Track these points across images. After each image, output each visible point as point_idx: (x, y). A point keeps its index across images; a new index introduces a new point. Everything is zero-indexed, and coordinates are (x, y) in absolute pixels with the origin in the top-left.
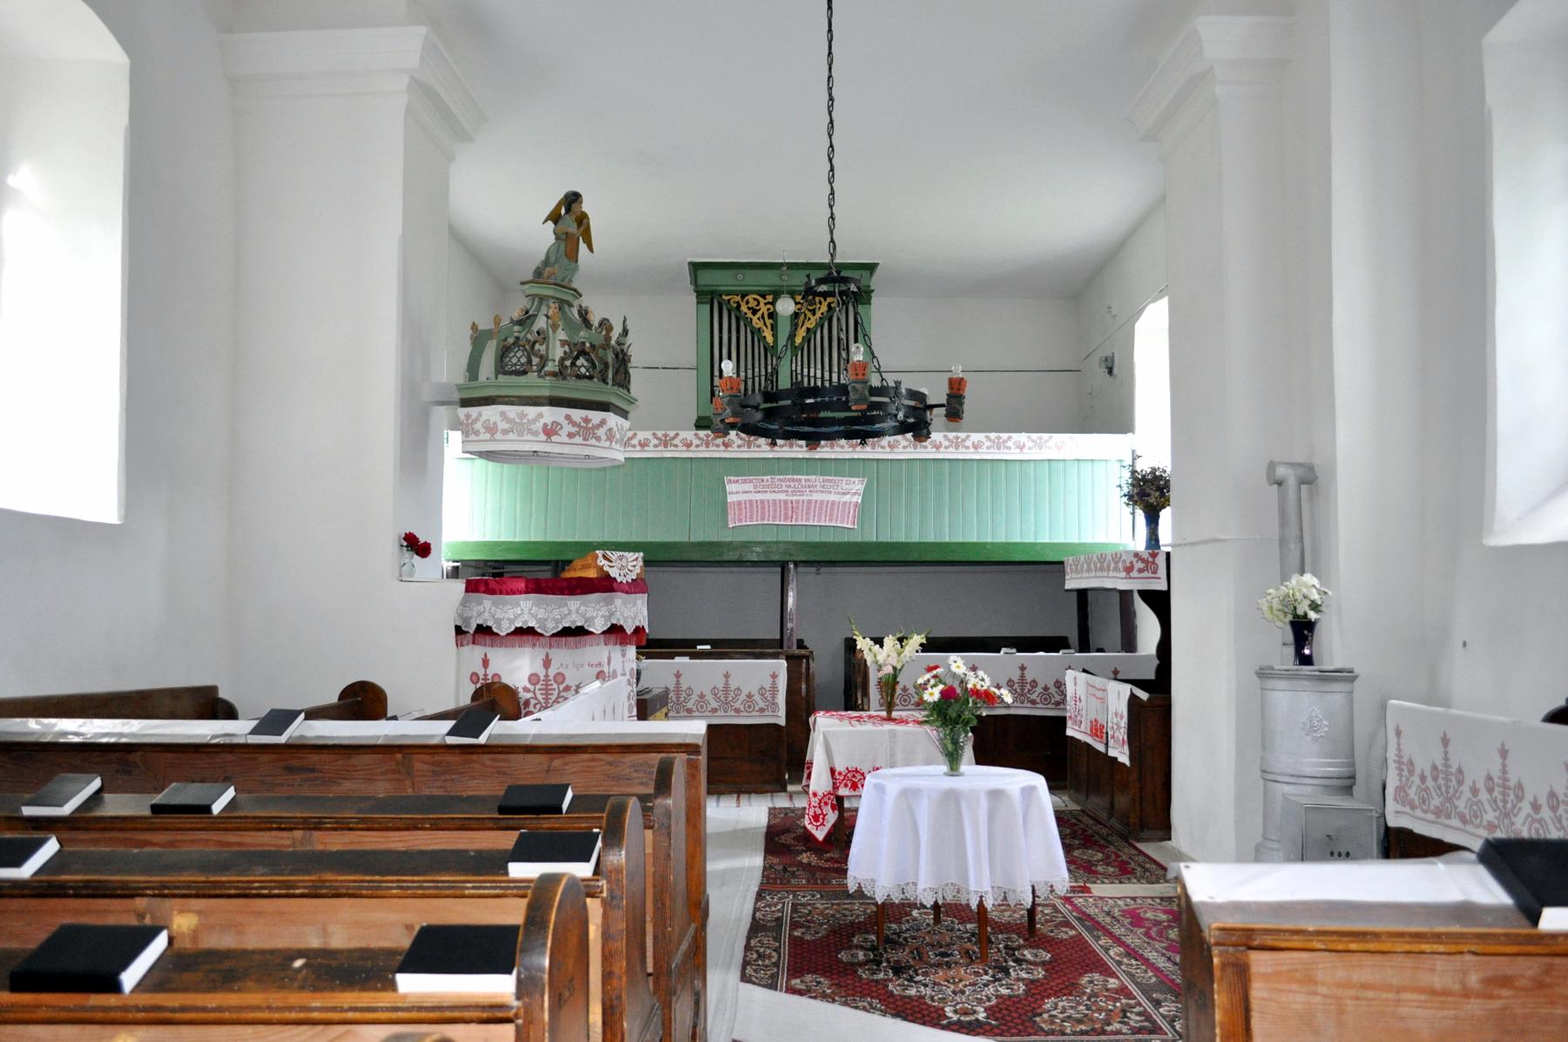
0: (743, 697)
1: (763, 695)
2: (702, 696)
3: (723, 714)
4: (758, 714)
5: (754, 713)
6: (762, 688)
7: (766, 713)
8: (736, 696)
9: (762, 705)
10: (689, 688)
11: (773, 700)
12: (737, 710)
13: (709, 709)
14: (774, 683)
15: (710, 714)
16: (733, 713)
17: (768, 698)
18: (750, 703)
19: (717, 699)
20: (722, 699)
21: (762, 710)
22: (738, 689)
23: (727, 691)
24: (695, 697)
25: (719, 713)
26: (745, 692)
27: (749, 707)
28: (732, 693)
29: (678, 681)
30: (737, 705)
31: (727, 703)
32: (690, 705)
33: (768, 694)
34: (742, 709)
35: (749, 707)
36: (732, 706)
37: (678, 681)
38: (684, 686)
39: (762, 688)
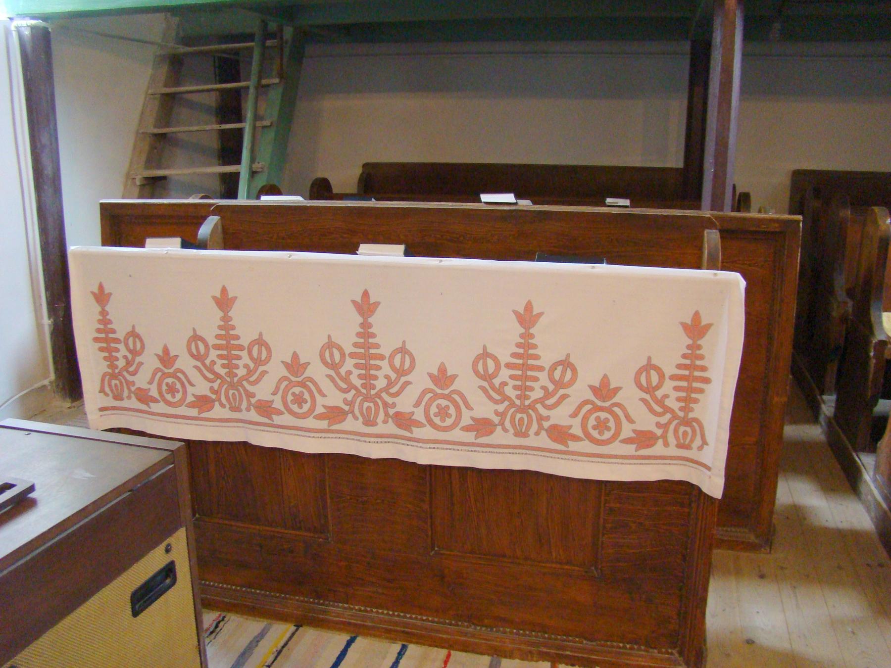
0: (579, 392)
1: (649, 390)
2: (442, 378)
3: (509, 439)
4: (630, 449)
5: (617, 448)
6: (649, 367)
7: (658, 449)
8: (559, 384)
9: (646, 421)
10: (403, 350)
11: (686, 409)
12: (559, 434)
13: (466, 420)
14: (693, 355)
15: (470, 437)
16: (543, 441)
17: (673, 403)
18: (603, 415)
19: (494, 392)
20: (510, 391)
21: (644, 439)
22: (566, 363)
23: (525, 367)
24: (420, 381)
25: (498, 437)
26: (589, 376)
27: (601, 426)
28: (543, 377)
29: (366, 325)
30: (560, 416)
31: (523, 409)
32: (405, 403)
33: (668, 386)
34: (577, 431)
35: (601, 426)
36: (541, 418)
37: (366, 325)
38: (386, 343)
39: (649, 367)
